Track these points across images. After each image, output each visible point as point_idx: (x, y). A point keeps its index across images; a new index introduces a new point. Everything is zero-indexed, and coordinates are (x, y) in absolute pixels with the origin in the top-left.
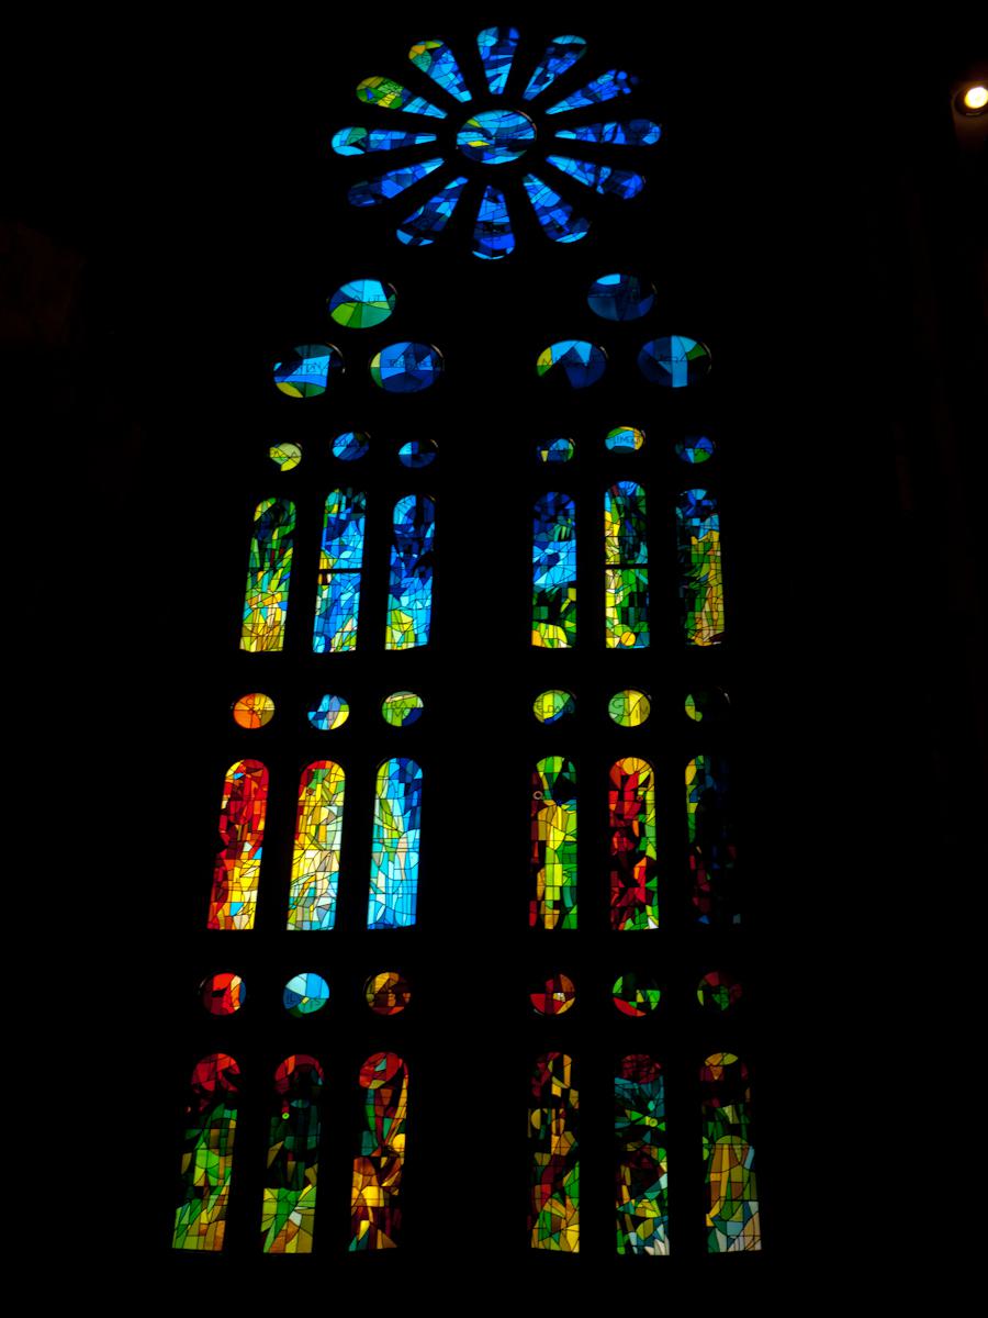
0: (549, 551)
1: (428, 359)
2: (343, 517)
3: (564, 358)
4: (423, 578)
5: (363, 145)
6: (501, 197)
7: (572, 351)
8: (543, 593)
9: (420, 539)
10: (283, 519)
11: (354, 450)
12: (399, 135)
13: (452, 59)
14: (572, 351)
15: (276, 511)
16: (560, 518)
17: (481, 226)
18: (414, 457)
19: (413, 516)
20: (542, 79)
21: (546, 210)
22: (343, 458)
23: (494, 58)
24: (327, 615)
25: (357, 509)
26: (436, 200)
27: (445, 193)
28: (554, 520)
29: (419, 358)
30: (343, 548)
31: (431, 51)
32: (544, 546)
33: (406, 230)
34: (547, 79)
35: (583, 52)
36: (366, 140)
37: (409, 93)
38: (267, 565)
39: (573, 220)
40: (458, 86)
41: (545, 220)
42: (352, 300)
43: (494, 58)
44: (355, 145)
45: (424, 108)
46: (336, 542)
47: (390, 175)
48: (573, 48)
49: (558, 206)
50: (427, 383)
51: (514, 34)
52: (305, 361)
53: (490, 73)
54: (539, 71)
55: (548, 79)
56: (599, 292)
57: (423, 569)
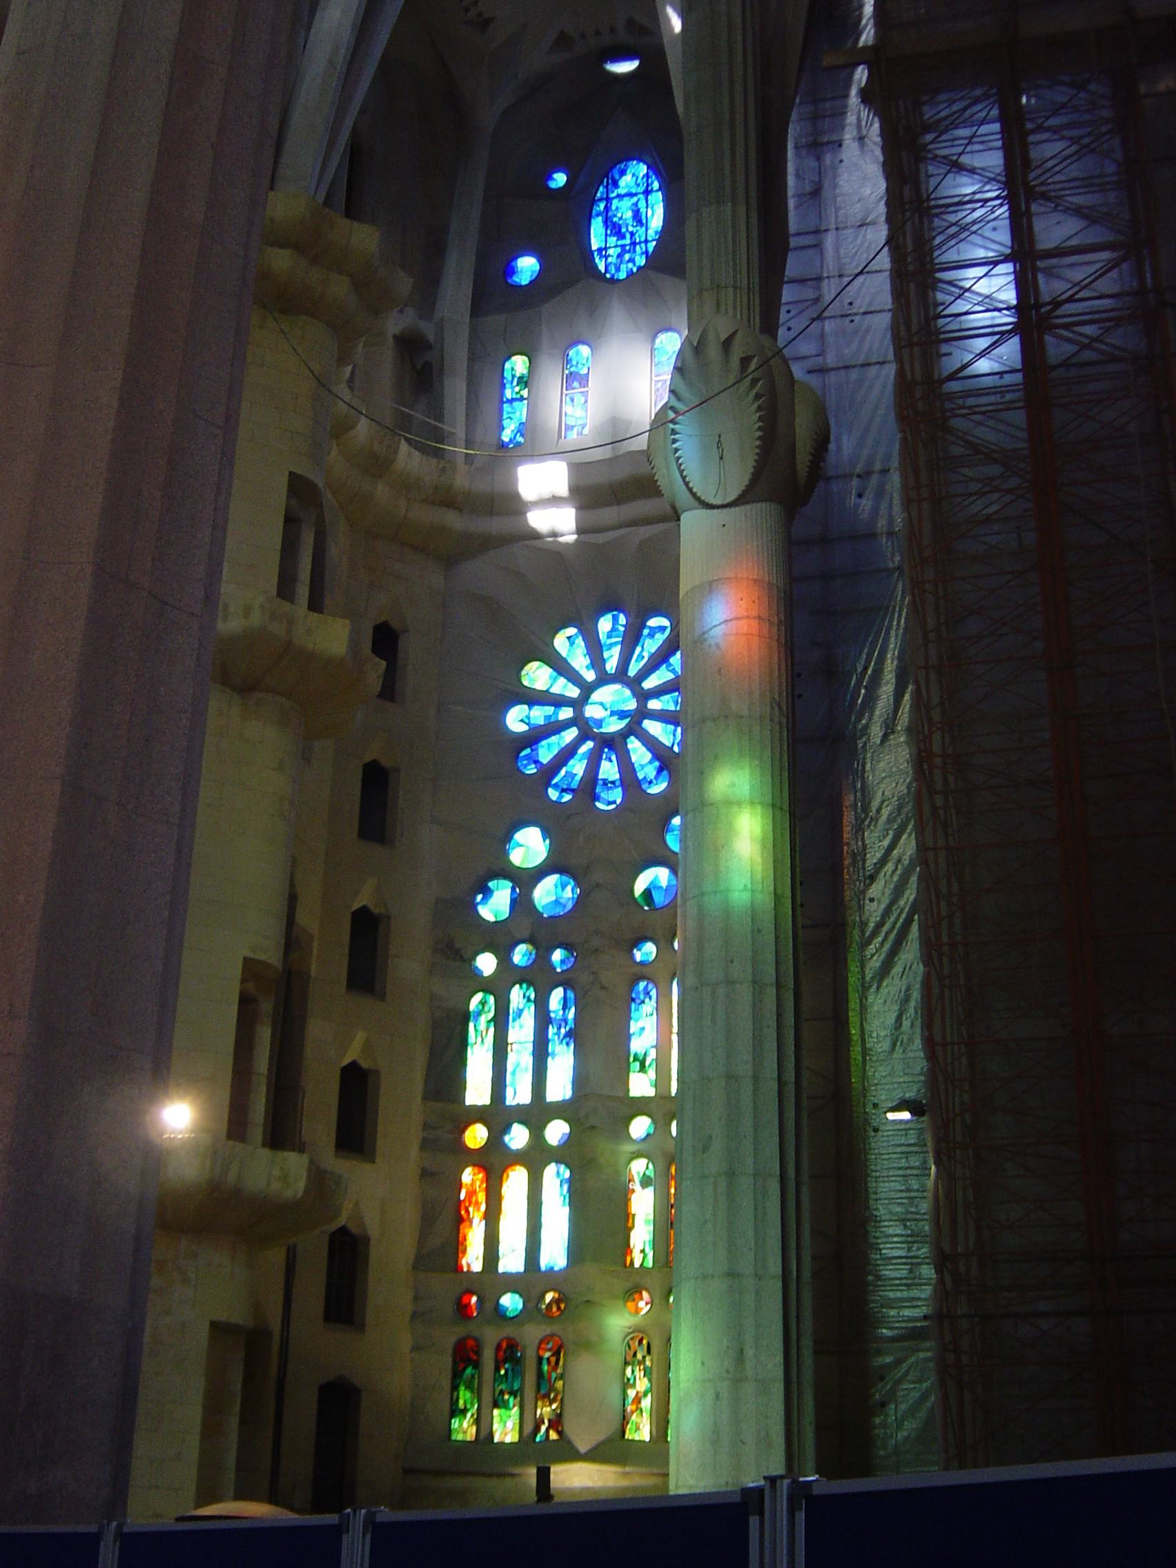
0: (640, 1024)
1: (569, 888)
2: (521, 1007)
3: (652, 882)
4: (568, 1044)
5: (527, 721)
6: (614, 758)
7: (657, 876)
8: (635, 1055)
9: (566, 1021)
10: (486, 1009)
11: (526, 958)
12: (549, 710)
13: (583, 644)
14: (657, 876)
15: (483, 1003)
16: (647, 1000)
17: (600, 782)
18: (562, 962)
19: (562, 1002)
20: (641, 657)
21: (642, 767)
22: (520, 964)
23: (609, 641)
24: (514, 1073)
25: (529, 1000)
26: (571, 762)
27: (577, 757)
28: (643, 1002)
29: (564, 887)
30: (521, 1027)
31: (569, 638)
32: (637, 1020)
33: (556, 786)
34: (643, 657)
35: (668, 631)
36: (528, 717)
37: (555, 674)
38: (479, 1039)
39: (660, 771)
40: (587, 667)
41: (640, 776)
42: (522, 846)
43: (609, 641)
44: (522, 721)
45: (565, 687)
46: (517, 1022)
47: (544, 743)
48: (663, 629)
49: (650, 762)
50: (570, 905)
51: (622, 619)
52: (495, 893)
53: (606, 655)
54: (638, 649)
55: (643, 657)
56: (673, 831)
57: (568, 1039)
